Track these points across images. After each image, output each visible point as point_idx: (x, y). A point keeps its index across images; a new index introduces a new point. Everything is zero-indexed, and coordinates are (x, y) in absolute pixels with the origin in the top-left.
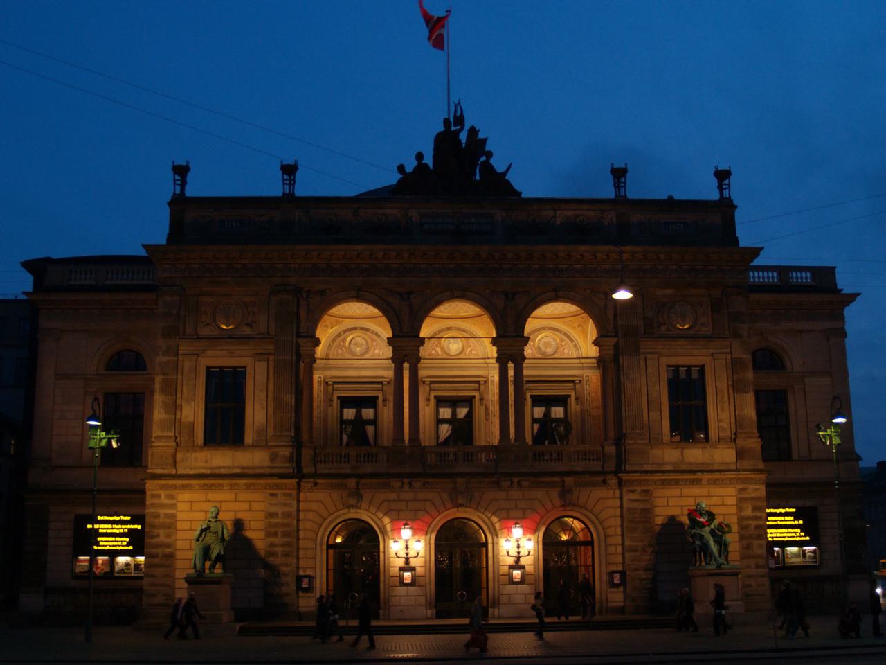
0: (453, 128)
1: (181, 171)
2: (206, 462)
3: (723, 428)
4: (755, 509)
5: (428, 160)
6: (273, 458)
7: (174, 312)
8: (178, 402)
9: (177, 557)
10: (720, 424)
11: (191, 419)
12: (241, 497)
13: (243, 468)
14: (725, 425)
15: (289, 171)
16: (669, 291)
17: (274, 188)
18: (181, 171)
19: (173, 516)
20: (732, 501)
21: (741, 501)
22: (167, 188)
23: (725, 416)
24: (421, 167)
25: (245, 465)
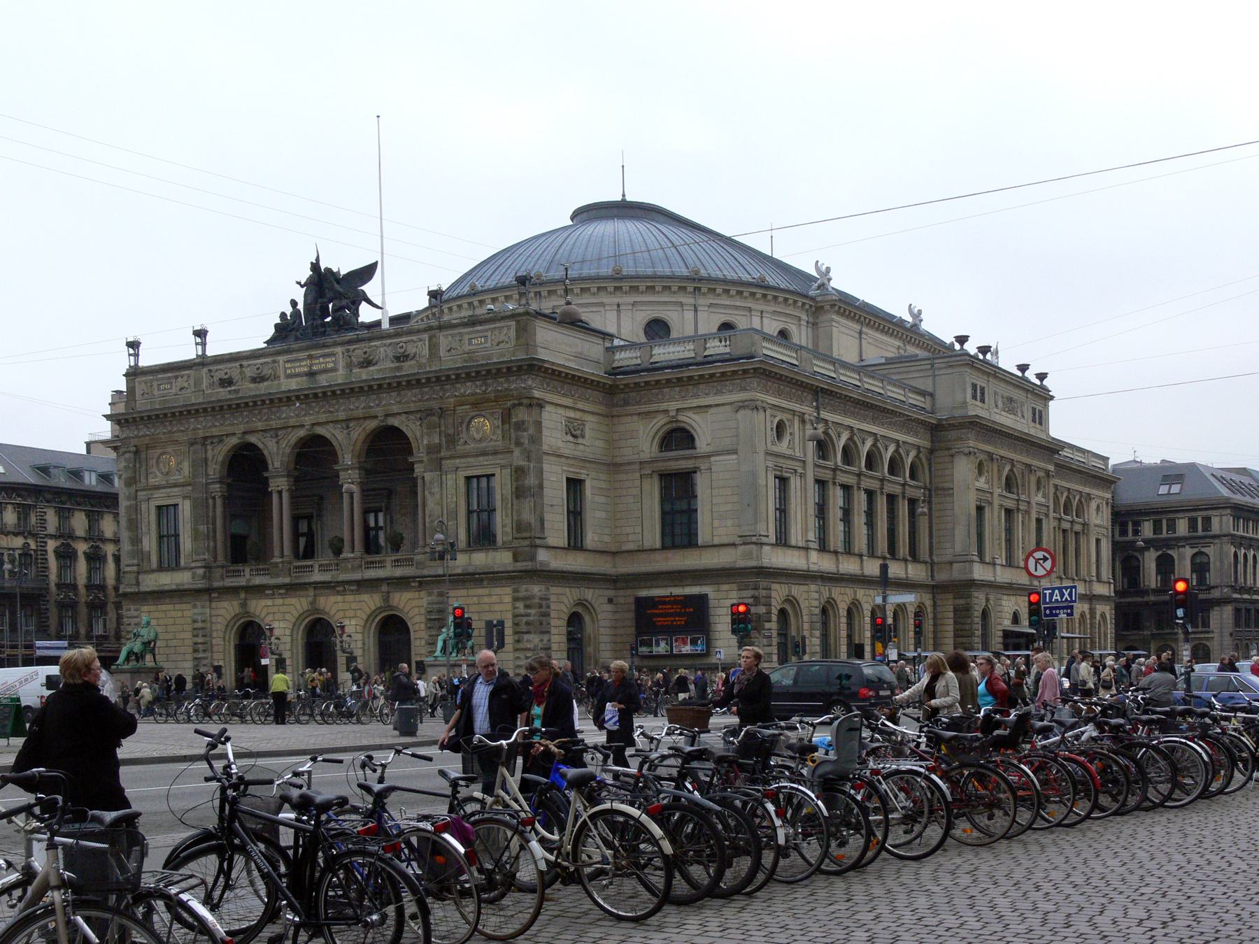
3: (507, 533)
4: (527, 607)
5: (301, 307)
14: (508, 529)
15: (201, 334)
17: (188, 352)
18: (134, 345)
20: (508, 599)
21: (516, 599)
22: (124, 362)
23: (508, 521)
24: (296, 313)
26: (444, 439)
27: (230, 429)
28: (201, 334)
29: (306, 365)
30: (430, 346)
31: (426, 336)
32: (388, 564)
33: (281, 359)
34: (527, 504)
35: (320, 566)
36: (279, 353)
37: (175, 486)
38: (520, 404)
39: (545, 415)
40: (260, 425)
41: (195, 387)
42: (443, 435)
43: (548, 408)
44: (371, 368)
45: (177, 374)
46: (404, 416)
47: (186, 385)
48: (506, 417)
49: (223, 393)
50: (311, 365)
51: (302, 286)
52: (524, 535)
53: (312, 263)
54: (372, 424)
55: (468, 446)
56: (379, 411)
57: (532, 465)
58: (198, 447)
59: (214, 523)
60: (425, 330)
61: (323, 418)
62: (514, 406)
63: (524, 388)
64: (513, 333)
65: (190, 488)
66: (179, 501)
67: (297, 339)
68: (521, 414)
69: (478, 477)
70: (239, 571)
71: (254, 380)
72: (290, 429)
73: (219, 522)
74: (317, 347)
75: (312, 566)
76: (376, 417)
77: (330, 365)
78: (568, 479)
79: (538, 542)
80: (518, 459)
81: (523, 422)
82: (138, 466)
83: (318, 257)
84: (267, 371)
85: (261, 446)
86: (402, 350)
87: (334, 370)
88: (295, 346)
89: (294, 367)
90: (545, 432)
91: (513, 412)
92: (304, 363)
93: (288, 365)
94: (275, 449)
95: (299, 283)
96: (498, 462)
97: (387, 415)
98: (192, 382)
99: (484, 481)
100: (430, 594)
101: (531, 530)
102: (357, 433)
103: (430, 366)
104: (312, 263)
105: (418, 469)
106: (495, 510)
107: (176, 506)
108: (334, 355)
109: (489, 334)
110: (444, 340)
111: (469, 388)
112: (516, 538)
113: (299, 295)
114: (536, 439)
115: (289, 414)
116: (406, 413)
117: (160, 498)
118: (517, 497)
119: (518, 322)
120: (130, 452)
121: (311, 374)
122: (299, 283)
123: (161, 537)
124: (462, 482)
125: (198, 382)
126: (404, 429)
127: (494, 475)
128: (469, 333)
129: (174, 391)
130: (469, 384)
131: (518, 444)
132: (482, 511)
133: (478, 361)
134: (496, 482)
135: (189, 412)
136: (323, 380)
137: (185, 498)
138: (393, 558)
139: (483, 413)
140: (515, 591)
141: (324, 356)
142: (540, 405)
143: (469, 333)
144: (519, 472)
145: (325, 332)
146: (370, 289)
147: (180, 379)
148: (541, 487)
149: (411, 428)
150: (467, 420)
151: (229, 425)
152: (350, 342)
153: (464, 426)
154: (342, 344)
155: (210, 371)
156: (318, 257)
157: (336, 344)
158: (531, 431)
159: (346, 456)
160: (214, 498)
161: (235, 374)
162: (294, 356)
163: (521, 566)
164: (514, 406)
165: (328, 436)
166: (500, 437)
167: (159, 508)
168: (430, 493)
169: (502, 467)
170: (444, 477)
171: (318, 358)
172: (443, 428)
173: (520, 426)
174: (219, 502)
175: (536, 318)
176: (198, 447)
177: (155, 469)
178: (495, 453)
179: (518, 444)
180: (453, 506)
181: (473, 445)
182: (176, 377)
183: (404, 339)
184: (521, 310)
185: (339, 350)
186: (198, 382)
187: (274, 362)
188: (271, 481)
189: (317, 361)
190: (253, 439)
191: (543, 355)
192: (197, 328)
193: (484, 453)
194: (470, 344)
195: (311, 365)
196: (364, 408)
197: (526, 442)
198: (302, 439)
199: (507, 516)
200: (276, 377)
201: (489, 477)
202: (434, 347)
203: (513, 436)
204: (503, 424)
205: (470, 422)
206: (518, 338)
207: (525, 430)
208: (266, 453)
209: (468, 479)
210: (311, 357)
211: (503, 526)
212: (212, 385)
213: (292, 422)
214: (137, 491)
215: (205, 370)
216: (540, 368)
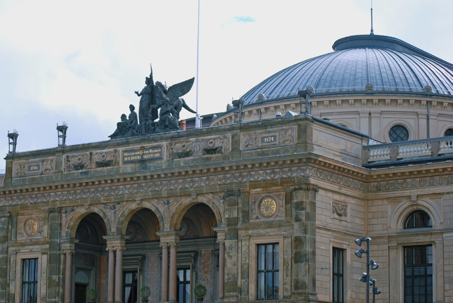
1: (13, 136)
3: (287, 290)
7: (5, 227)
8: (8, 281)
10: (285, 286)
11: (13, 292)
14: (288, 287)
15: (62, 129)
16: (259, 190)
18: (13, 136)
23: (288, 280)
24: (133, 115)
26: (240, 214)
28: (62, 129)
29: (139, 155)
30: (232, 142)
31: (229, 135)
33: (120, 149)
34: (303, 266)
36: (119, 145)
37: (37, 243)
38: (300, 189)
39: (318, 197)
41: (56, 169)
42: (240, 211)
43: (321, 192)
44: (187, 158)
45: (44, 158)
46: (211, 195)
47: (49, 167)
48: (289, 199)
50: (143, 154)
51: (139, 95)
52: (300, 291)
53: (147, 78)
54: (187, 201)
55: (258, 220)
57: (308, 236)
58: (57, 214)
59: (64, 274)
60: (229, 130)
62: (295, 189)
63: (303, 176)
64: (295, 134)
65: (47, 246)
66: (38, 255)
67: (133, 135)
68: (299, 197)
69: (266, 245)
71: (100, 164)
72: (125, 203)
73: (68, 273)
74: (149, 140)
77: (157, 155)
78: (334, 248)
79: (311, 297)
80: (297, 231)
81: (302, 203)
82: (10, 227)
83: (152, 74)
86: (211, 145)
87: (160, 158)
88: (131, 139)
89: (130, 156)
90: (318, 211)
91: (294, 193)
92: (138, 153)
93: (126, 154)
94: (113, 219)
95: (137, 93)
96: (282, 233)
97: (198, 195)
98: (54, 165)
99: (270, 248)
101: (306, 287)
102: (175, 208)
103: (232, 158)
104: (147, 78)
105: (220, 237)
106: (278, 271)
107: (36, 259)
108: (160, 147)
109: (277, 134)
110: (243, 138)
112: (294, 294)
113: (136, 102)
114: (311, 217)
117: (25, 253)
118: (296, 262)
119: (299, 125)
120: (5, 217)
121: (142, 161)
122: (137, 93)
123: (23, 283)
124: (253, 249)
125: (58, 165)
127: (278, 243)
129: (40, 171)
130: (261, 172)
131: (298, 220)
132: (268, 271)
133: (268, 155)
134: (279, 249)
135: (51, 187)
137: (43, 253)
139: (271, 195)
141: (153, 148)
142: (315, 189)
143: (261, 134)
144: (298, 242)
145: (154, 129)
146: (188, 98)
147: (45, 163)
148: (314, 253)
150: (259, 199)
152: (172, 138)
153: (257, 204)
154: (166, 139)
155: (68, 157)
156: (152, 74)
157: (162, 139)
158: (308, 209)
159: (166, 225)
160: (65, 254)
161: (85, 160)
162: (131, 147)
164: (295, 189)
165: (153, 209)
166: (284, 214)
167: (24, 260)
168: (229, 256)
169: (285, 237)
170: (240, 244)
171: (148, 149)
172: (240, 206)
173: (300, 206)
174: (69, 257)
175: (313, 122)
176: (57, 214)
177: (22, 231)
178: (280, 225)
179: (298, 220)
180: (246, 267)
181: (263, 220)
182: (43, 161)
183: (213, 137)
184: (302, 116)
186: (58, 165)
187: (116, 151)
188: (108, 242)
189: (147, 152)
191: (317, 151)
193: (270, 225)
194: (263, 141)
195: (143, 154)
197: (304, 218)
198: (133, 210)
199: (287, 275)
200: (117, 163)
201: (274, 244)
202: (235, 142)
203: (294, 213)
204: (286, 203)
205: (261, 202)
206: (299, 138)
207: (303, 209)
208: (105, 221)
209: (258, 245)
210: (143, 148)
211: (284, 284)
214: (8, 247)
215: (64, 156)
216: (316, 160)
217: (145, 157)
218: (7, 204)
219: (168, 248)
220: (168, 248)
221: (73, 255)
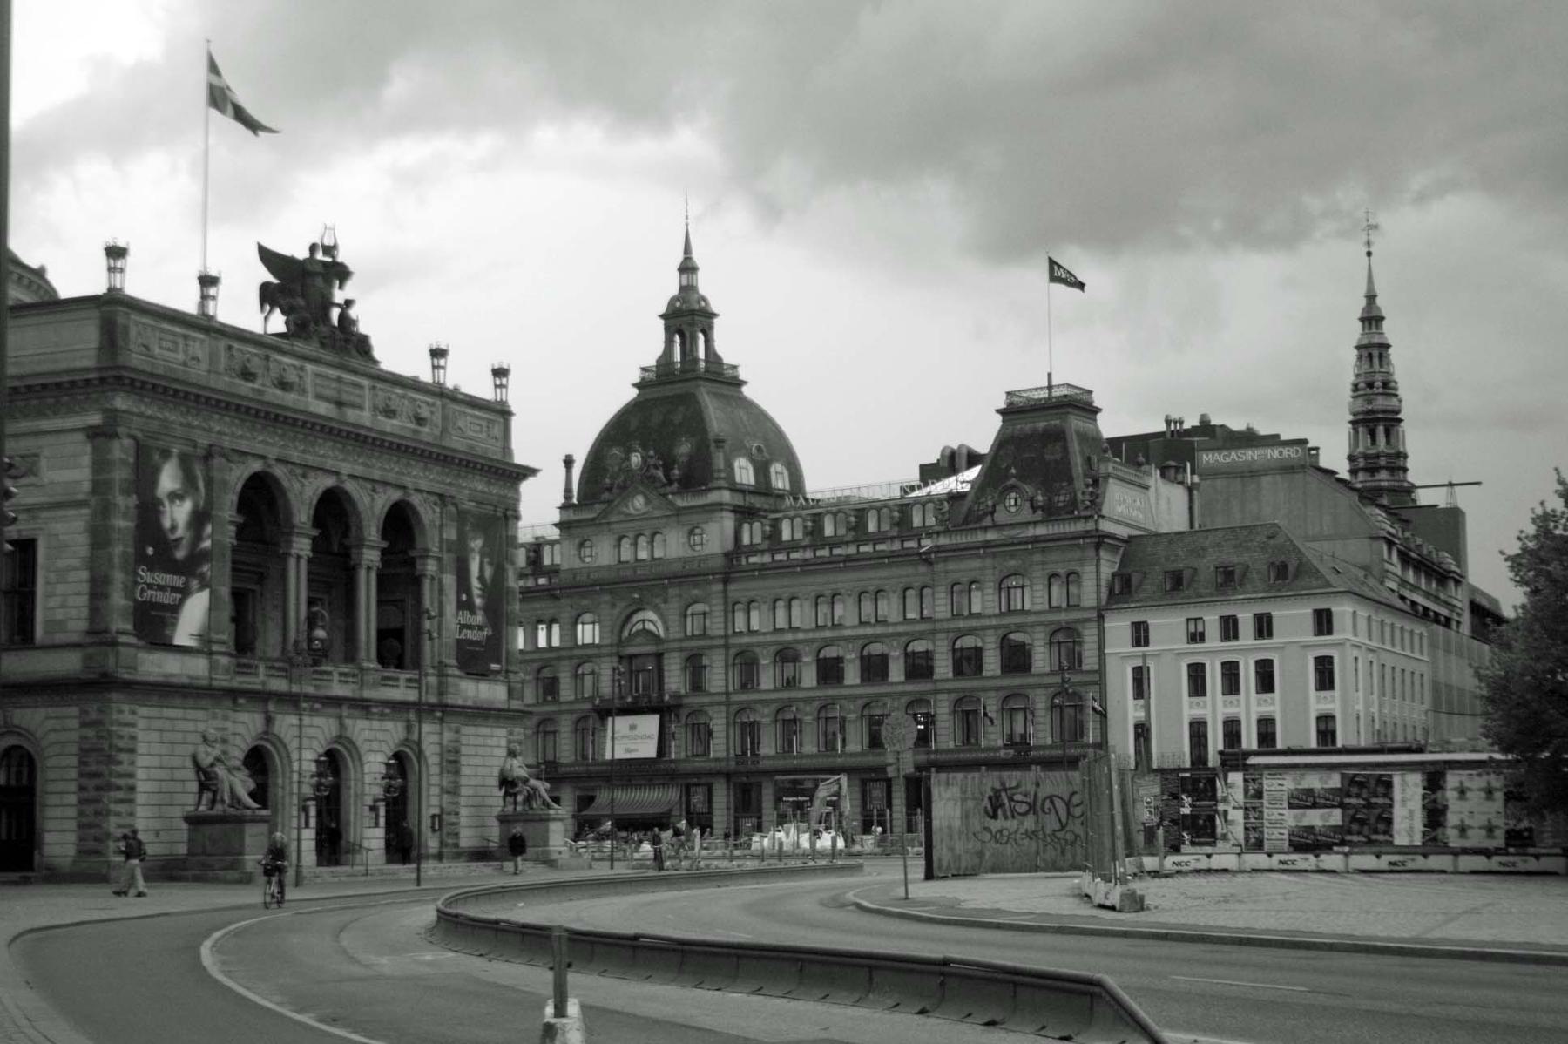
0: (320, 256)
2: (160, 667)
6: (213, 667)
9: (138, 789)
12: (191, 714)
13: (191, 677)
19: (133, 738)
25: (191, 673)
27: (260, 449)
28: (207, 281)
32: (402, 683)
33: (310, 367)
35: (341, 674)
40: (295, 456)
49: (245, 387)
56: (408, 481)
61: (359, 470)
70: (249, 666)
72: (320, 473)
75: (330, 673)
76: (404, 488)
84: (292, 377)
85: (285, 484)
100: (450, 729)
108: (360, 387)
111: (480, 485)
115: (326, 453)
116: (428, 492)
126: (421, 510)
128: (472, 416)
129: (181, 357)
136: (351, 415)
138: (408, 676)
140: (511, 733)
143: (472, 416)
149: (428, 513)
151: (262, 442)
163: (515, 704)
165: (355, 495)
185: (366, 382)
190: (279, 471)
192: (213, 272)
196: (397, 473)
200: (303, 391)
212: (229, 370)
213: (329, 464)
217: (345, 397)
218: (135, 410)
219: (369, 568)
220: (369, 568)
221: (310, 561)
